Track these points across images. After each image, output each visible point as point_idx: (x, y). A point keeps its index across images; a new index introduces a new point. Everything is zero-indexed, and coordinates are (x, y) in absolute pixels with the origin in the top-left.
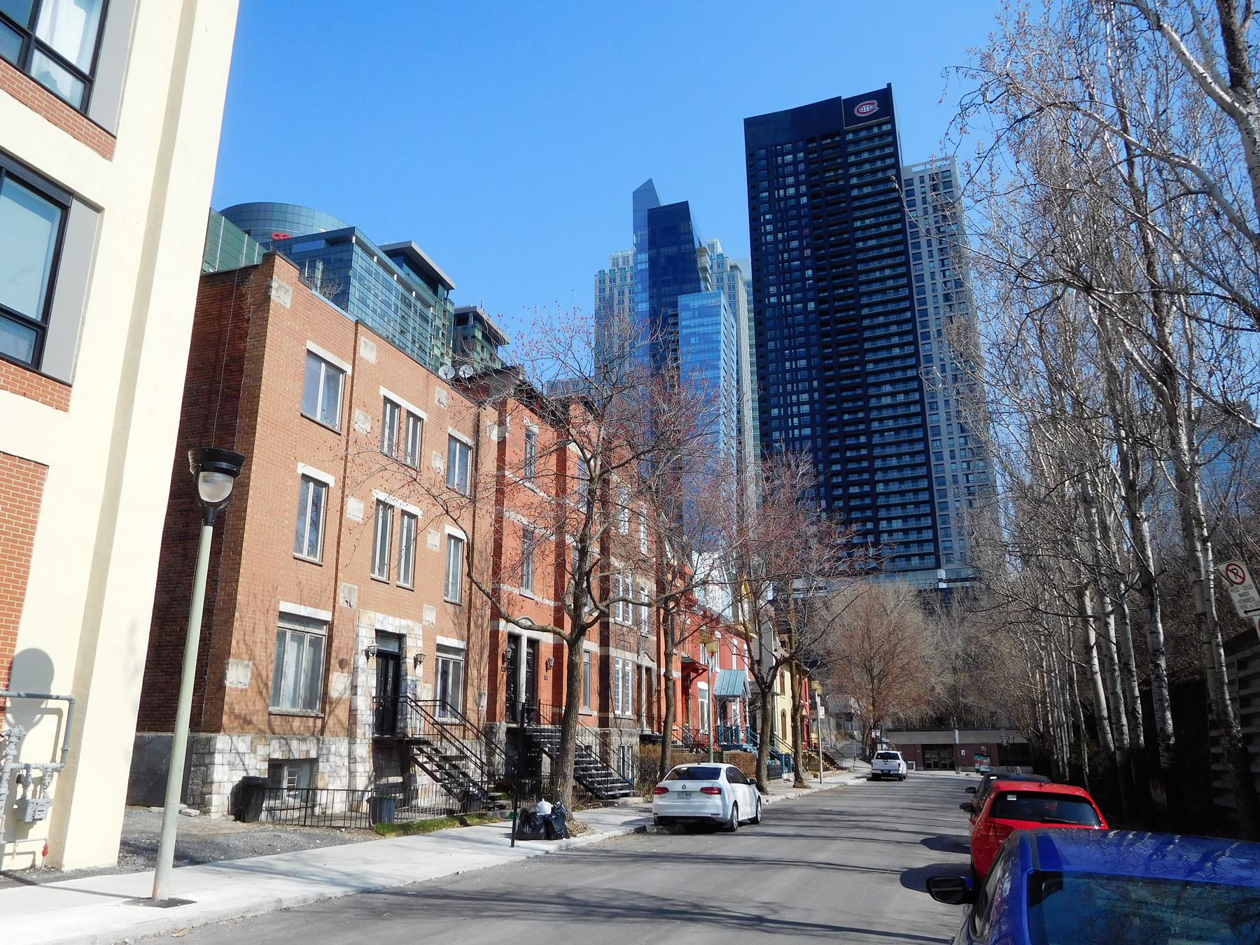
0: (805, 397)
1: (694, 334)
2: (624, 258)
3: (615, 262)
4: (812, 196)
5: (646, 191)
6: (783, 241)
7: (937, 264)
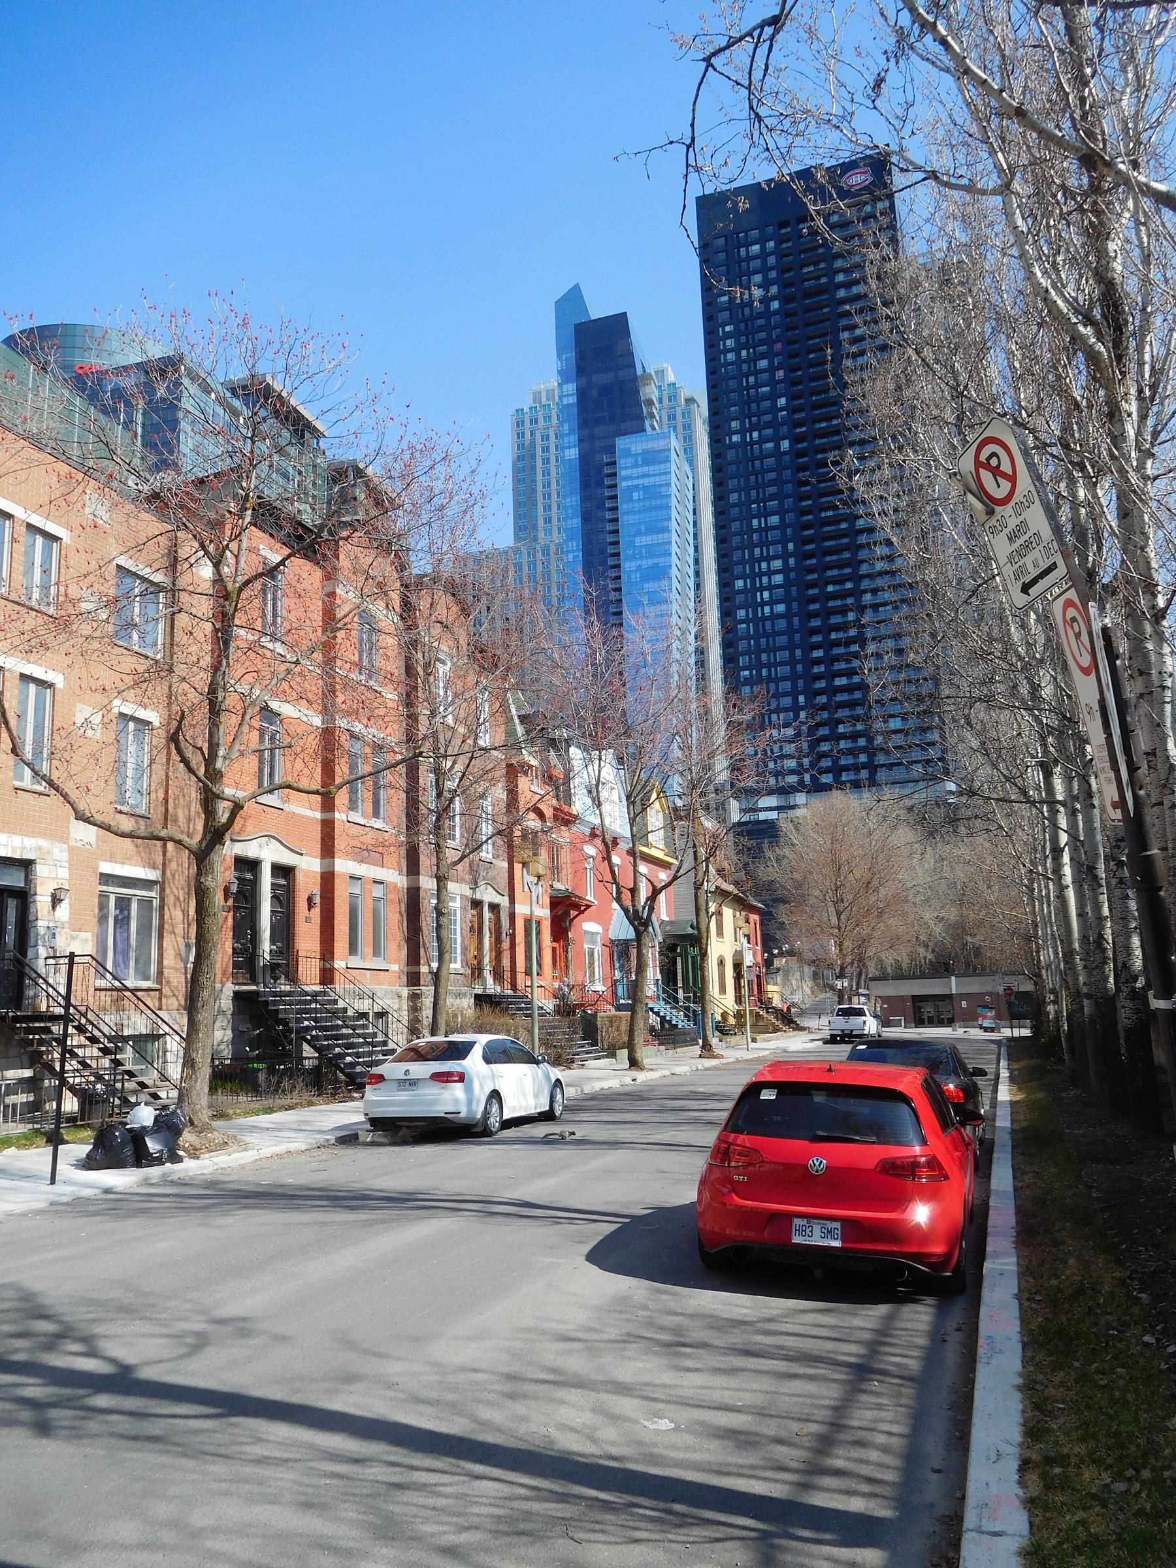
0: (777, 564)
1: (637, 486)
2: (548, 391)
3: (537, 397)
4: (785, 300)
5: (573, 299)
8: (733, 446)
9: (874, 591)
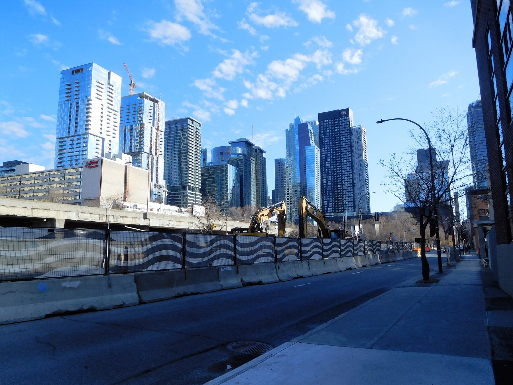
0: (330, 177)
2: (293, 125)
3: (290, 126)
4: (332, 132)
5: (297, 119)
6: (326, 142)
7: (357, 149)
8: (323, 157)
9: (345, 182)
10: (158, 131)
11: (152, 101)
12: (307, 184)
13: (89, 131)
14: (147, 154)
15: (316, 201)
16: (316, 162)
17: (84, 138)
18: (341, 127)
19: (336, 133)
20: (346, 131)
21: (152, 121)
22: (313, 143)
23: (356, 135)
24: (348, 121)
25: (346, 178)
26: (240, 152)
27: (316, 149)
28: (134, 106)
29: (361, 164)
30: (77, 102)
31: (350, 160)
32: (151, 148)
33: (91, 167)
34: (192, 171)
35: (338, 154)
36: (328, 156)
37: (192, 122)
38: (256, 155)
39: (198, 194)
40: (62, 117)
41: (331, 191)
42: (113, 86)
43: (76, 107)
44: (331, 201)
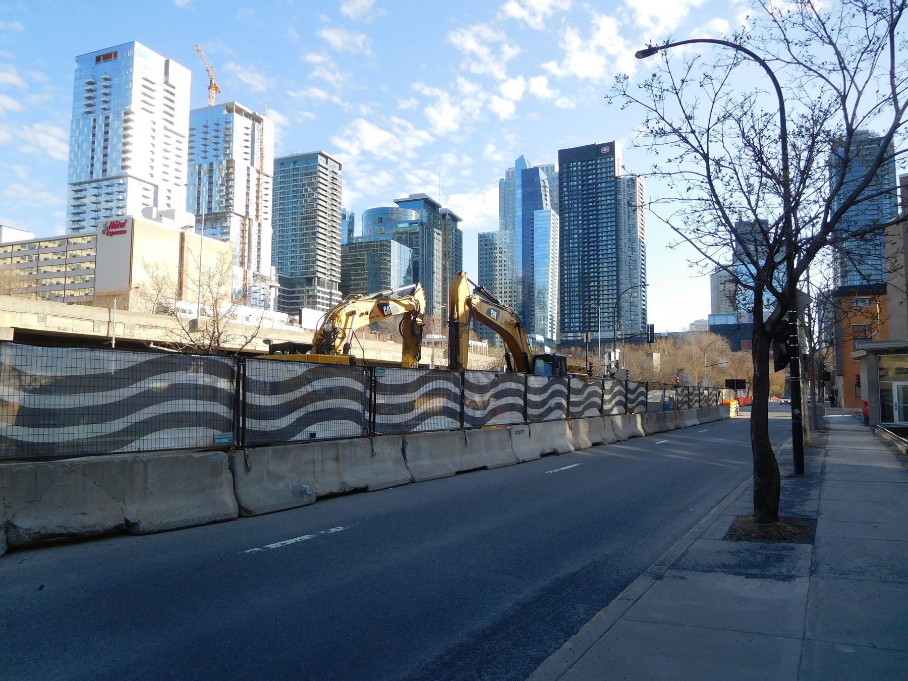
0: (577, 267)
3: (508, 174)
4: (583, 186)
7: (626, 217)
10: (261, 175)
11: (250, 118)
12: (535, 280)
13: (129, 171)
14: (239, 217)
15: (551, 309)
16: (551, 240)
17: (120, 184)
18: (599, 176)
19: (590, 187)
20: (608, 184)
21: (249, 157)
22: (547, 204)
23: (627, 191)
24: (612, 164)
25: (605, 269)
26: (414, 219)
27: (552, 217)
28: (216, 127)
29: (633, 244)
30: (106, 115)
31: (614, 237)
32: (247, 206)
33: (112, 234)
34: (325, 252)
35: (592, 226)
36: (574, 229)
37: (325, 159)
38: (445, 225)
39: (335, 294)
40: (78, 144)
41: (577, 293)
42: (174, 87)
43: (104, 125)
44: (577, 311)
